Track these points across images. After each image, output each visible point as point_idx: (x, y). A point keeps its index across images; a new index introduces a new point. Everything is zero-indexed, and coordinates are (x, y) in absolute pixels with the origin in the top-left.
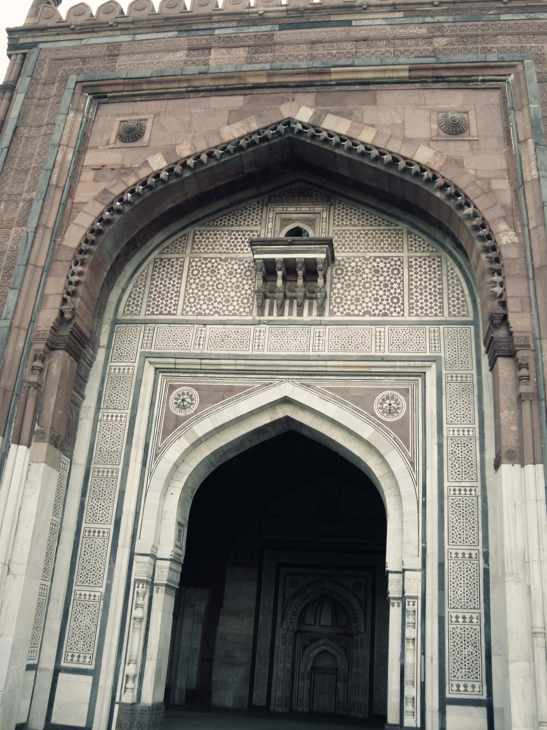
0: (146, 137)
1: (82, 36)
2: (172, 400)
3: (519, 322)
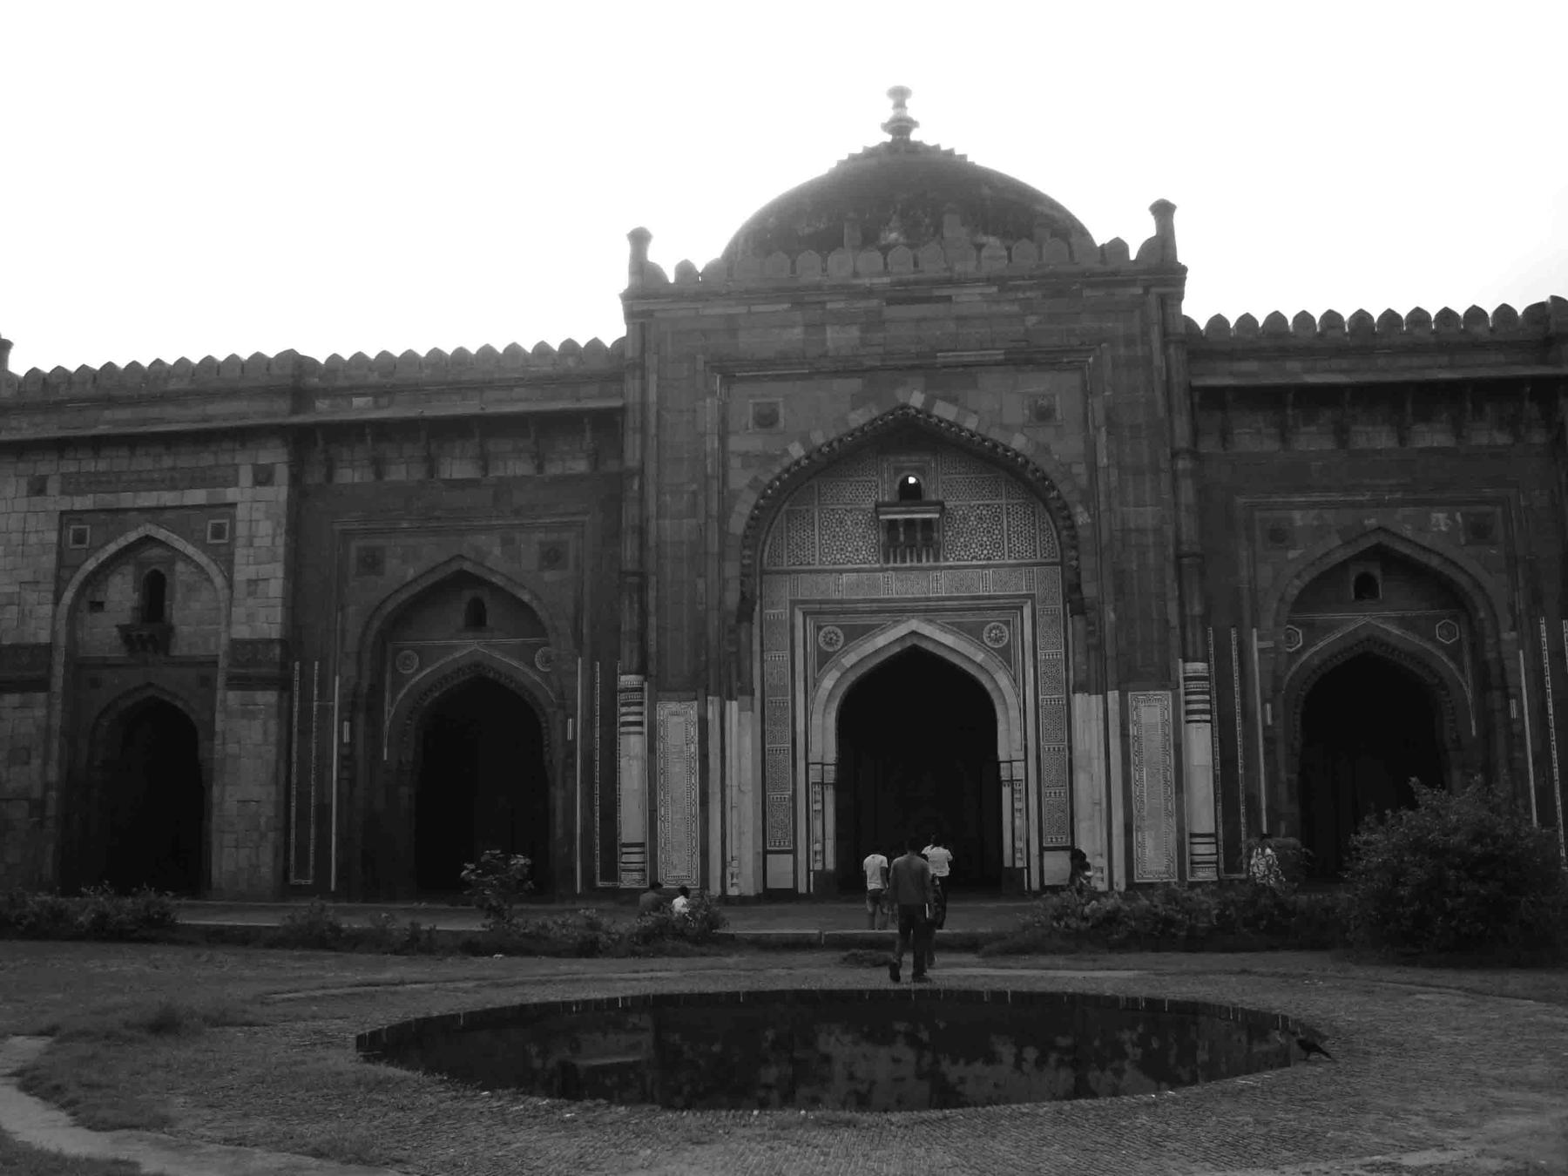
0: (782, 420)
1: (699, 305)
2: (821, 639)
3: (1089, 590)
